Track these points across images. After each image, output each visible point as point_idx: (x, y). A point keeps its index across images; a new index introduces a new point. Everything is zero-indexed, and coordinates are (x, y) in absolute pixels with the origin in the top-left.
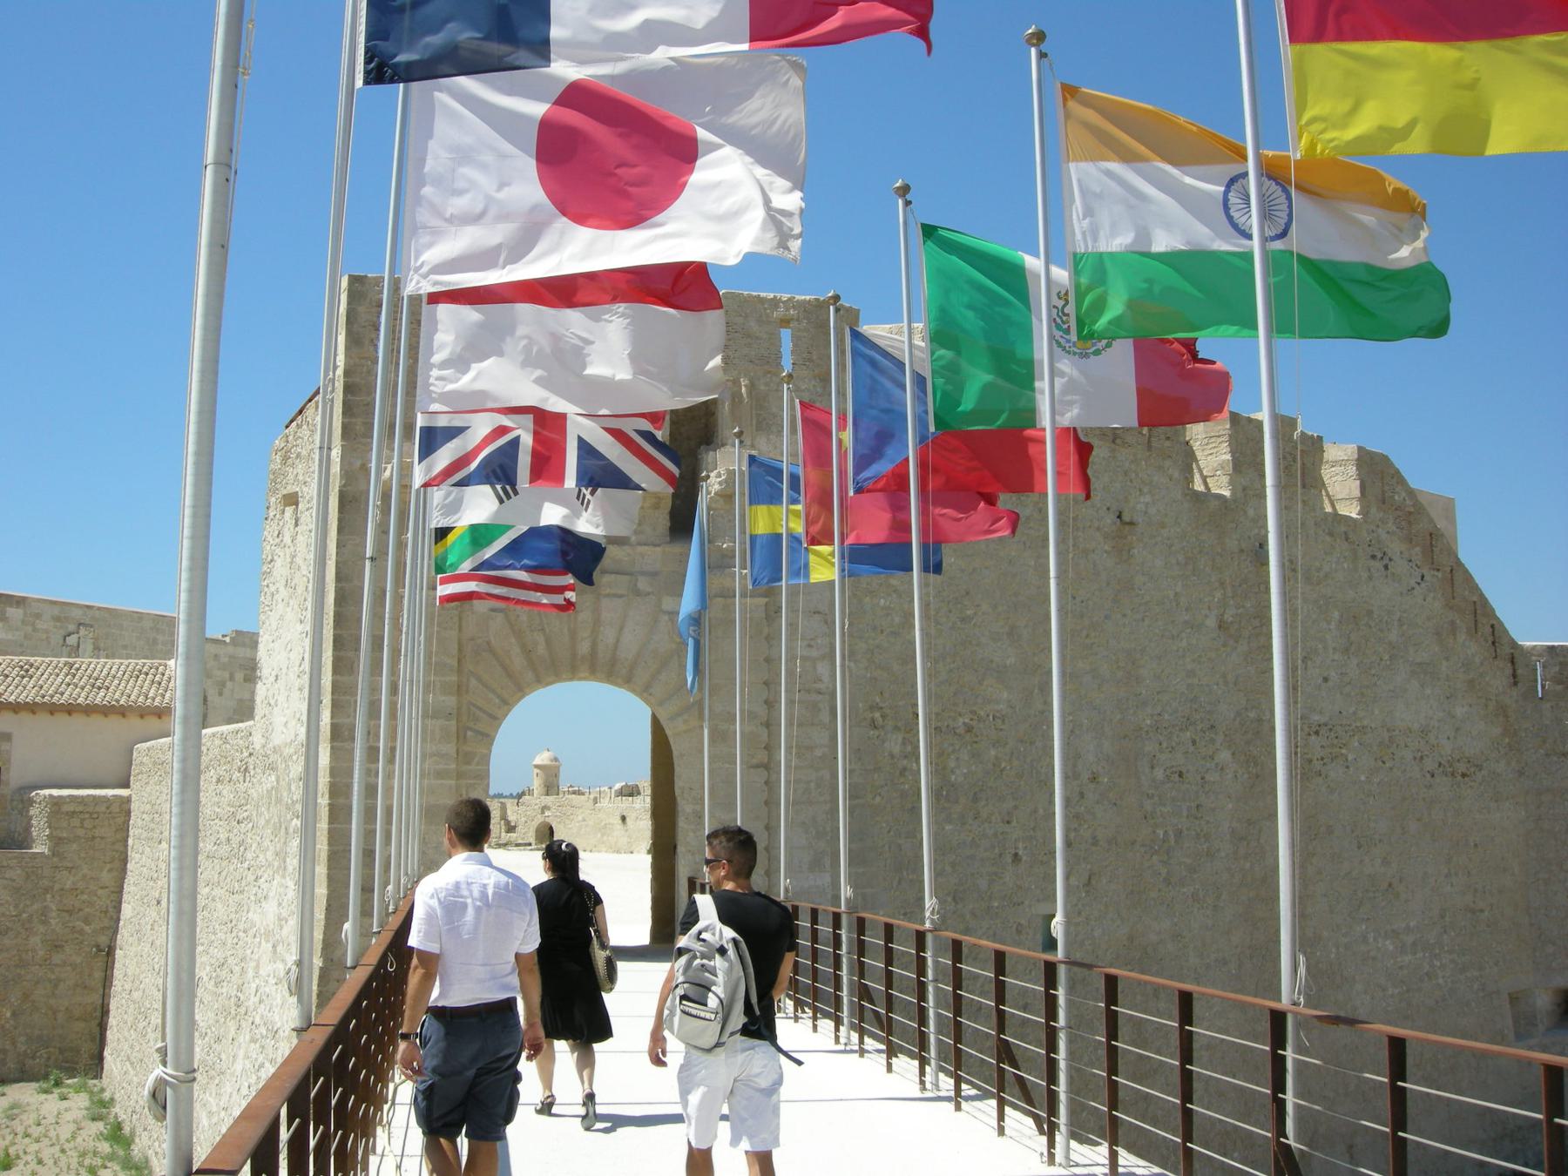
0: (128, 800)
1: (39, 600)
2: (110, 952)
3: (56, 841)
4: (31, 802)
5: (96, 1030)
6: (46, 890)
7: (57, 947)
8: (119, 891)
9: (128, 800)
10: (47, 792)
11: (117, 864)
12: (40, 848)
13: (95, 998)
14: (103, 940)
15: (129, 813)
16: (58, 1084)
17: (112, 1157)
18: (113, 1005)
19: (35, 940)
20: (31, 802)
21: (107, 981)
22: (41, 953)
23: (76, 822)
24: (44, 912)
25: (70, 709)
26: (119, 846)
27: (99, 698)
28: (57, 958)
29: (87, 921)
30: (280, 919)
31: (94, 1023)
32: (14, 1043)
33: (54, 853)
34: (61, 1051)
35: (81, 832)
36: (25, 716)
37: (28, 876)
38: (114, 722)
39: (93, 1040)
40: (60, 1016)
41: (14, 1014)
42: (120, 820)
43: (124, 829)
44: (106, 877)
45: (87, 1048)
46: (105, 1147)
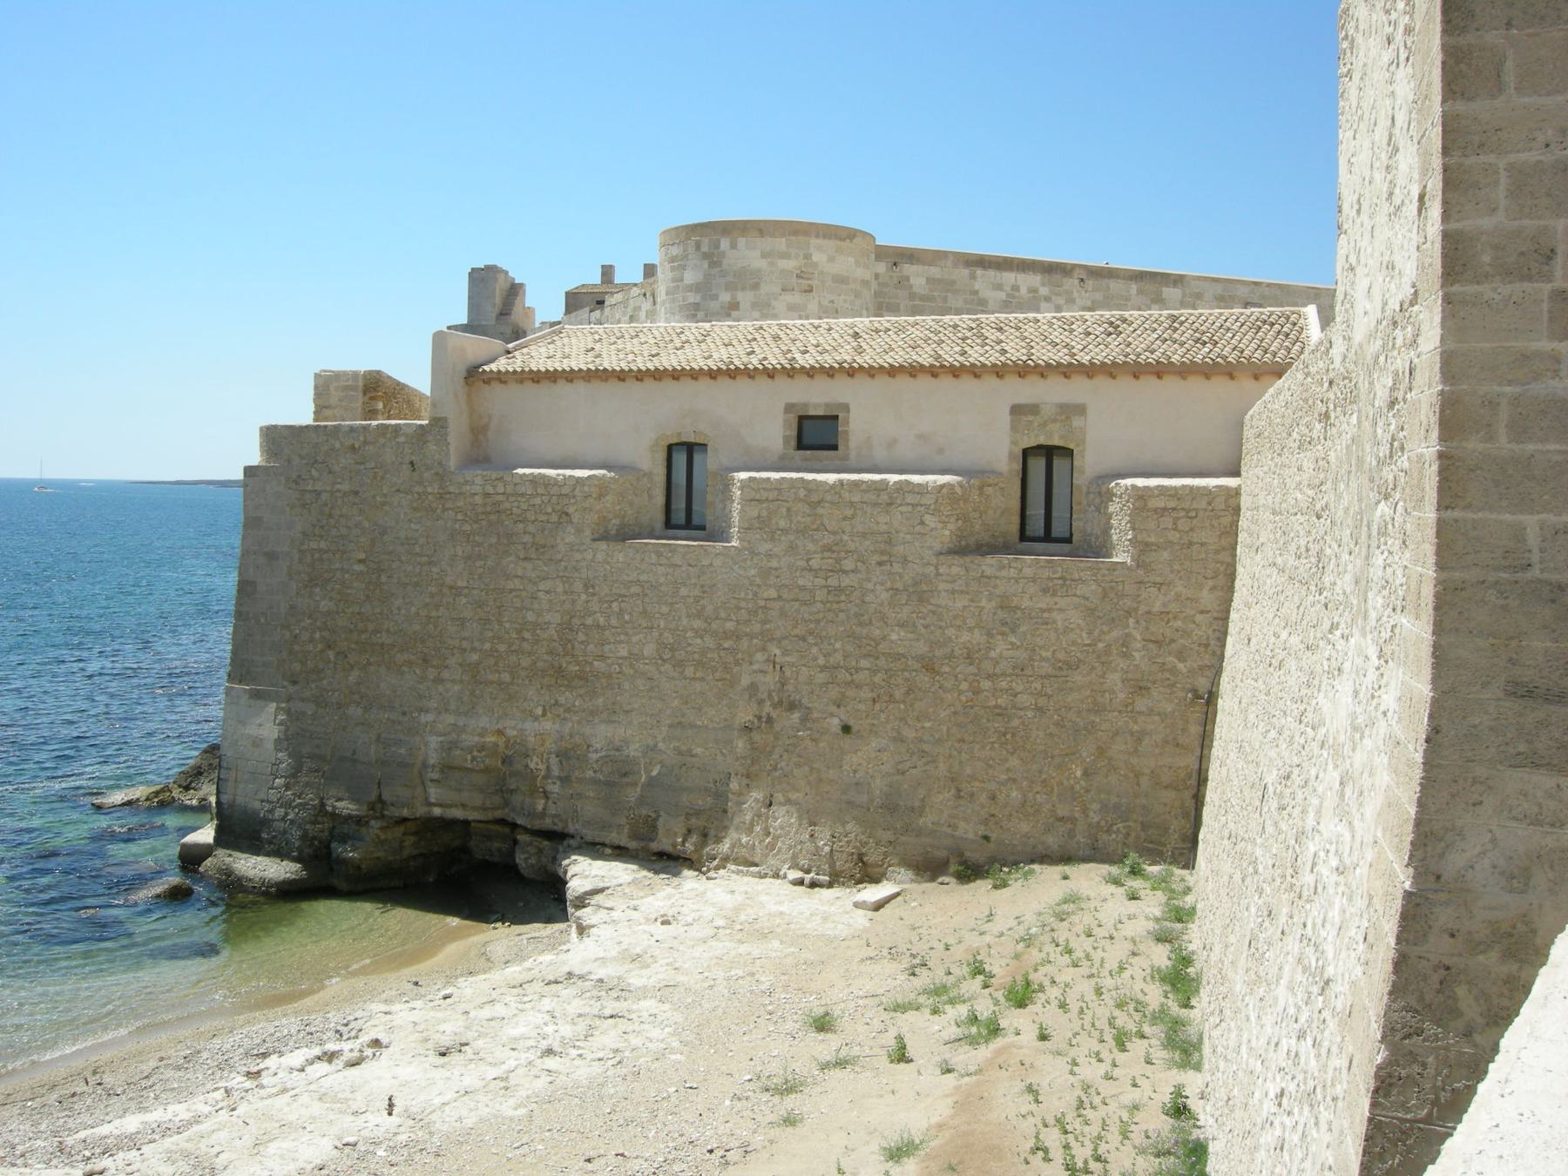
0: (1237, 492)
1: (1198, 278)
2: (1210, 700)
3: (1142, 548)
4: (1110, 495)
5: (1190, 803)
6: (1129, 613)
7: (1141, 689)
8: (1225, 619)
9: (1237, 492)
10: (1129, 482)
11: (1221, 580)
12: (1121, 557)
13: (1191, 761)
14: (1202, 684)
15: (1237, 510)
16: (1135, 872)
17: (1160, 1016)
18: (1214, 773)
19: (1114, 678)
20: (1110, 495)
21: (1206, 740)
22: (1122, 696)
23: (1167, 522)
24: (1126, 641)
25: (1160, 370)
26: (1225, 557)
27: (1201, 354)
28: (1141, 704)
29: (1181, 658)
30: (1355, 728)
31: (1188, 795)
32: (1085, 811)
33: (1139, 563)
34: (1144, 826)
35: (1174, 536)
36: (1101, 382)
37: (1105, 595)
38: (1220, 384)
39: (1186, 815)
40: (1144, 781)
41: (1086, 774)
42: (1226, 520)
43: (1231, 533)
44: (1207, 598)
45: (1177, 825)
46: (1155, 995)
